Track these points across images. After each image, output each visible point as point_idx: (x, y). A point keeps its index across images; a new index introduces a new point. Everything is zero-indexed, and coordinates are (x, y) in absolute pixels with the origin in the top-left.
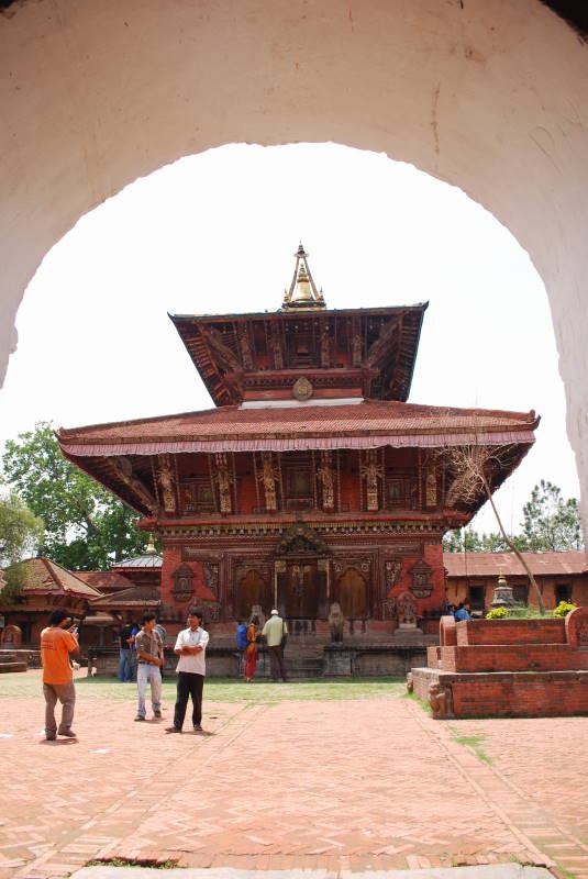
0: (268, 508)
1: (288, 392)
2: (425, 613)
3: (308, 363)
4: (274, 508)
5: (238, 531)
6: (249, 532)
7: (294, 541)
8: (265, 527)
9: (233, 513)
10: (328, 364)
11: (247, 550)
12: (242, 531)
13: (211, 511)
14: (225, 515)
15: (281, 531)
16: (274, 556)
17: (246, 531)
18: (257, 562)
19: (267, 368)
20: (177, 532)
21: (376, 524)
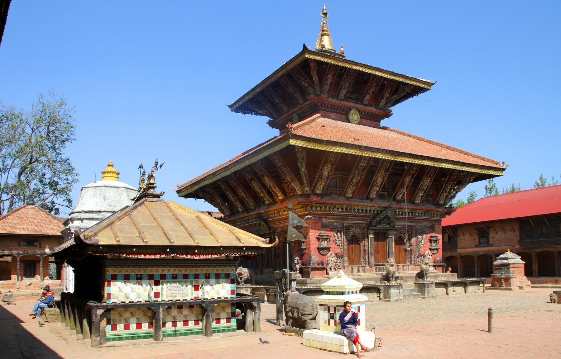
0: (371, 196)
1: (343, 116)
2: (435, 262)
3: (354, 99)
4: (374, 197)
5: (354, 209)
6: (360, 211)
7: (384, 218)
8: (368, 209)
9: (352, 198)
10: (366, 103)
11: (355, 222)
12: (356, 210)
13: (340, 195)
14: (348, 199)
15: (375, 212)
16: (369, 225)
17: (358, 210)
18: (358, 230)
19: (333, 97)
20: (321, 208)
21: (419, 211)
